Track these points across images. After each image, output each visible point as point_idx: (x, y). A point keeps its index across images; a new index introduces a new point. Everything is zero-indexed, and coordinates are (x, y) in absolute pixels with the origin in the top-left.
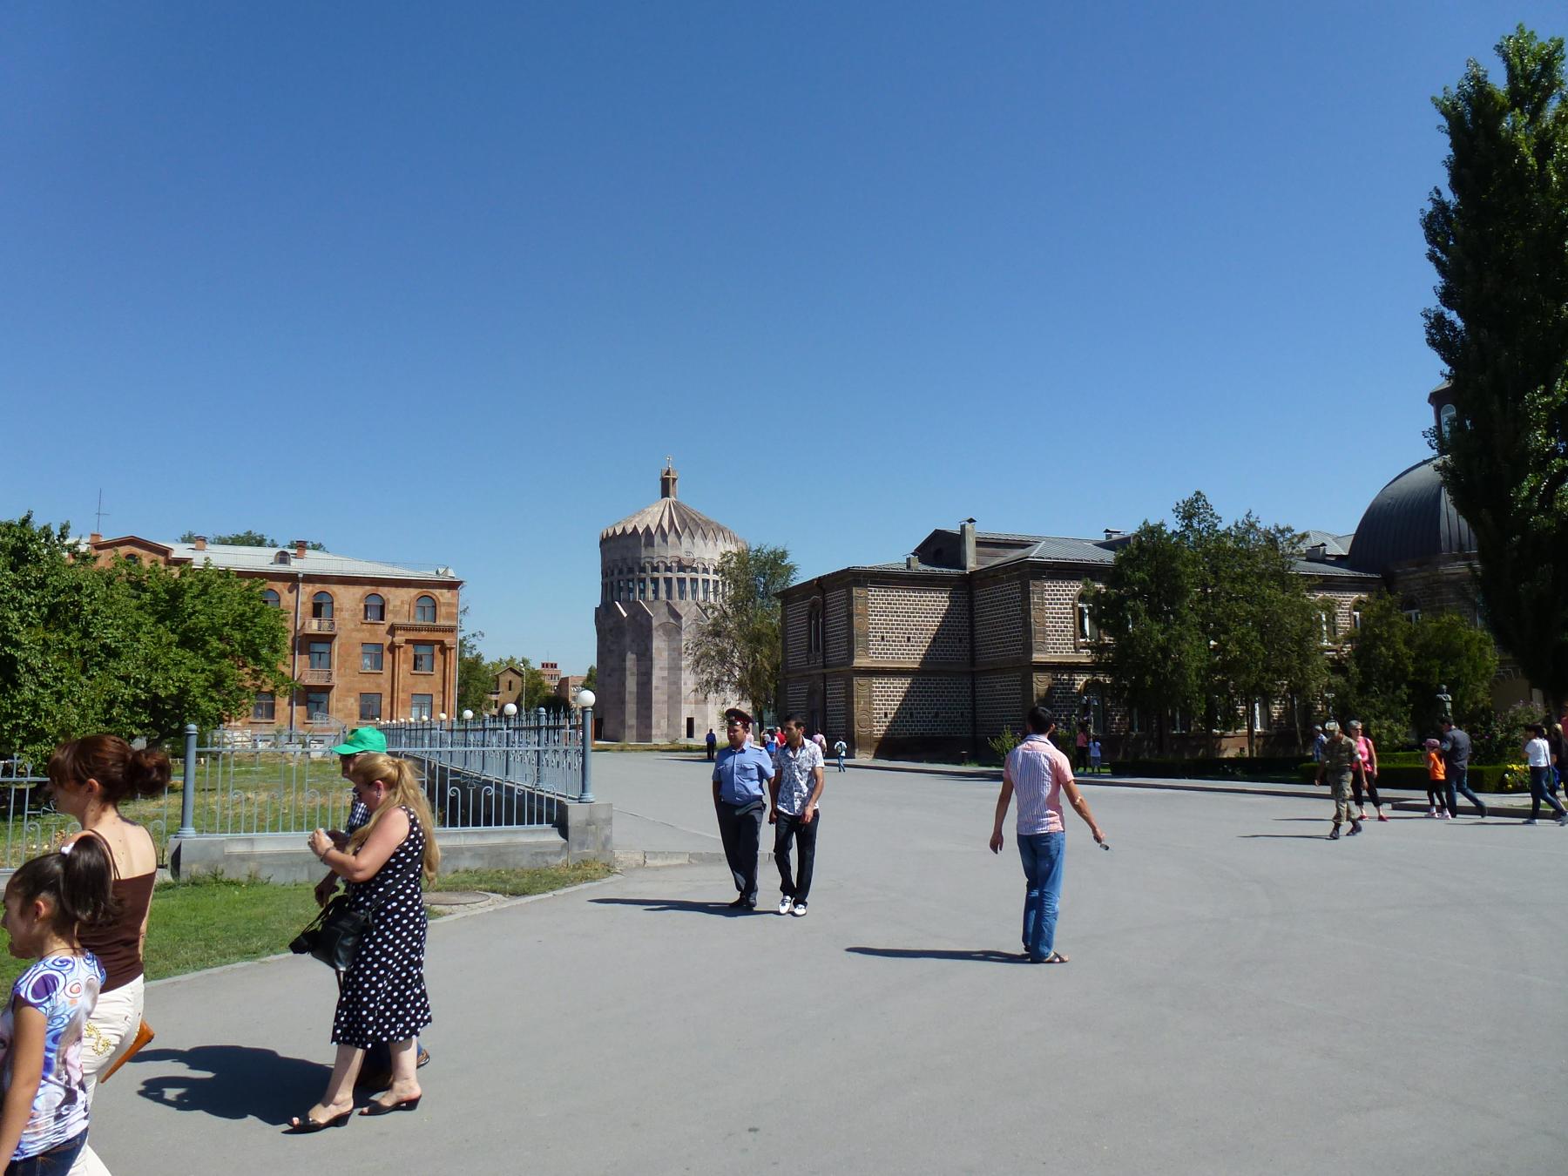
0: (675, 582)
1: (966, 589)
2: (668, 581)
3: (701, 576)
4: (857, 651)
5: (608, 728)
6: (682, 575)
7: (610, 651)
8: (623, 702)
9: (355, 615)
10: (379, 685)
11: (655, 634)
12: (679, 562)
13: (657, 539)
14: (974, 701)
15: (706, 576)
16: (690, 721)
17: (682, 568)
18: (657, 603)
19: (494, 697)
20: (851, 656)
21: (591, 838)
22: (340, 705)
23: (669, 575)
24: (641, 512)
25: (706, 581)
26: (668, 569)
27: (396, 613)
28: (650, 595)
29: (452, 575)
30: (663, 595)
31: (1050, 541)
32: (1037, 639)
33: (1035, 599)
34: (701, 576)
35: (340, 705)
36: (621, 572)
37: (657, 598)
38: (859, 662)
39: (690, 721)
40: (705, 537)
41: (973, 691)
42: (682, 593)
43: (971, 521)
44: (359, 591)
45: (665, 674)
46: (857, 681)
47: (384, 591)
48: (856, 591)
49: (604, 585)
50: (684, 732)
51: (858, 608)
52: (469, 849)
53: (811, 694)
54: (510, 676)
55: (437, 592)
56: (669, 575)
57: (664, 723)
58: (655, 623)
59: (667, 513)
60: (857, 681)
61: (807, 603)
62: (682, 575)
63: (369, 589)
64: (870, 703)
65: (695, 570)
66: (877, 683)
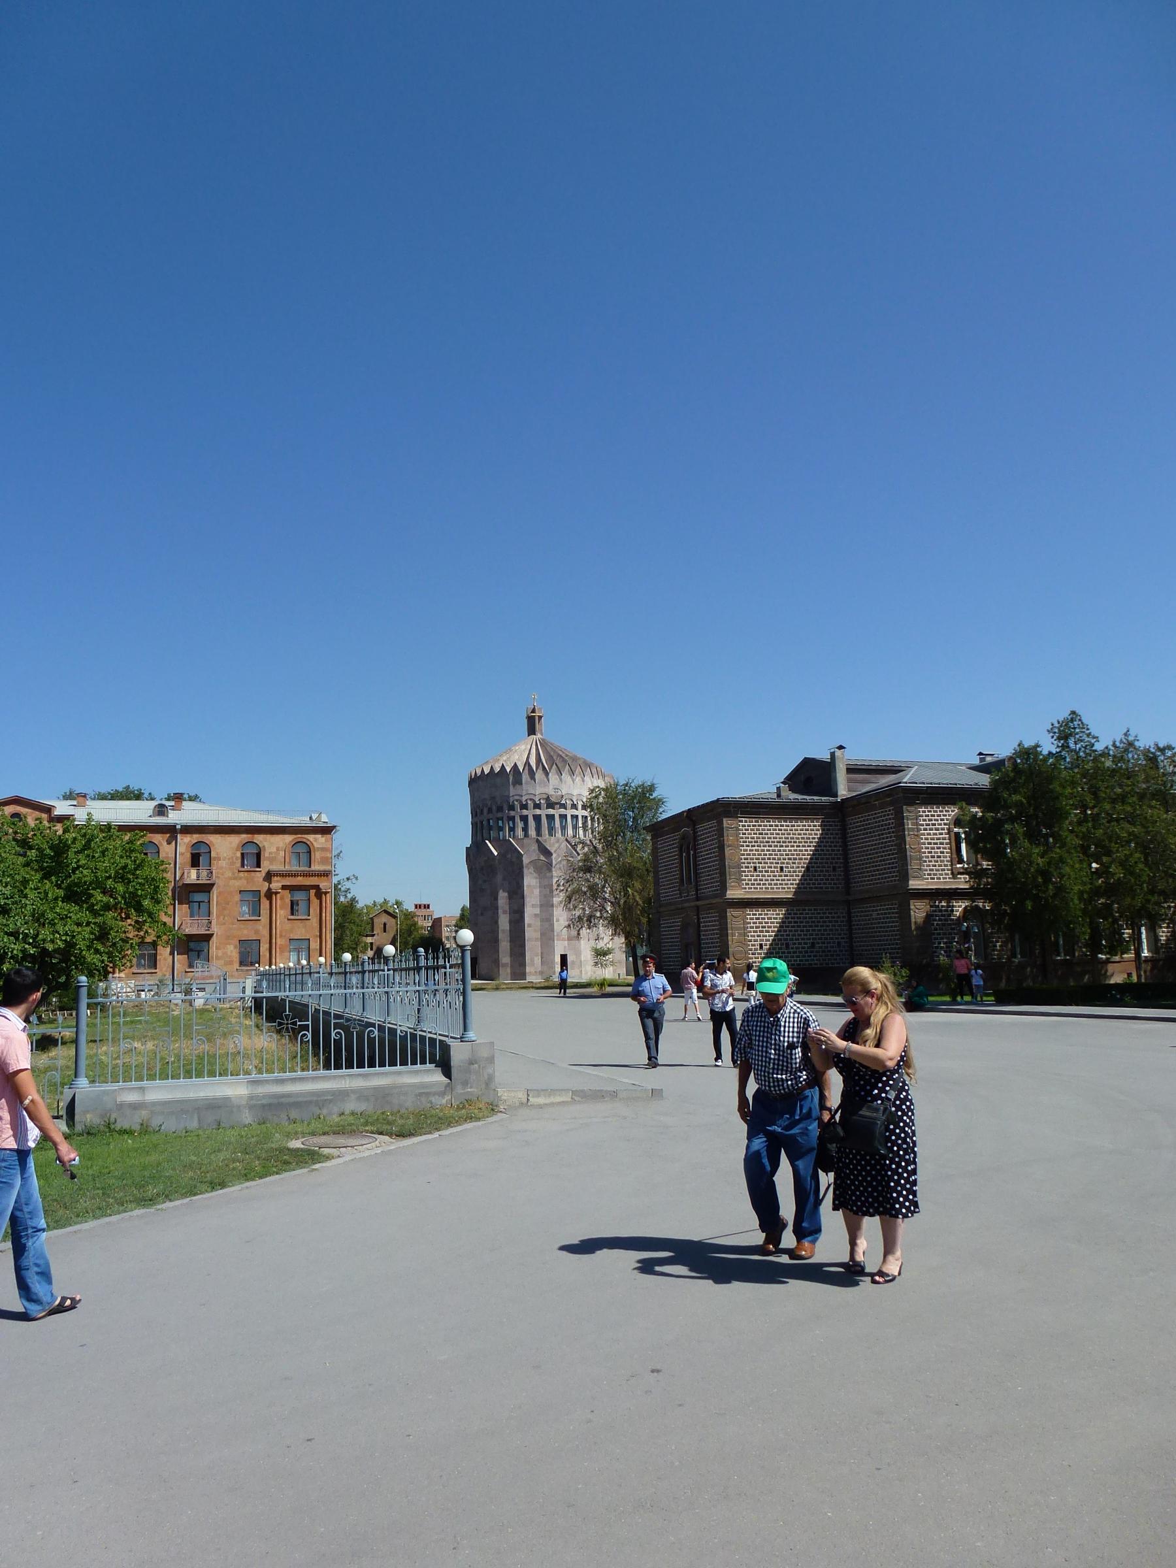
0: (544, 820)
1: (838, 817)
2: (537, 818)
3: (570, 812)
4: (730, 882)
5: (483, 967)
6: (551, 811)
8: (496, 941)
9: (233, 863)
10: (257, 932)
11: (525, 871)
12: (548, 799)
13: (525, 777)
14: (850, 930)
15: (575, 812)
16: (564, 958)
17: (551, 805)
18: (526, 841)
19: (369, 940)
20: (724, 888)
21: (473, 1077)
22: (220, 953)
23: (538, 812)
24: (509, 750)
25: (575, 817)
26: (537, 806)
27: (272, 860)
28: (520, 833)
29: (325, 819)
30: (532, 832)
31: (922, 765)
32: (913, 866)
33: (909, 825)
34: (570, 812)
35: (220, 953)
36: (490, 811)
37: (526, 835)
38: (733, 893)
39: (564, 958)
40: (572, 773)
41: (850, 921)
43: (841, 747)
44: (235, 840)
45: (537, 911)
46: (731, 913)
47: (259, 839)
48: (727, 822)
49: (474, 824)
51: (729, 839)
52: (354, 1091)
53: (685, 927)
54: (385, 918)
55: (311, 837)
56: (538, 812)
57: (537, 960)
58: (526, 860)
59: (534, 751)
60: (731, 913)
61: (677, 835)
62: (551, 811)
63: (245, 837)
64: (745, 935)
65: (564, 806)
66: (751, 914)
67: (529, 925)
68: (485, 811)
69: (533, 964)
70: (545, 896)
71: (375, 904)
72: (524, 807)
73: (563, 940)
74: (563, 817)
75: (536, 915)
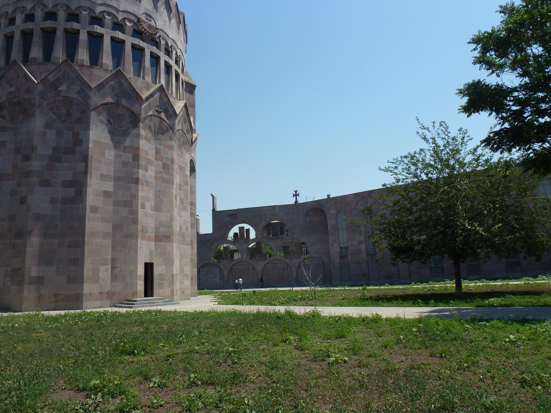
16: (149, 267)
26: (118, 26)
30: (107, 59)
34: (163, 58)
36: (30, 18)
39: (149, 267)
42: (139, 71)
45: (109, 186)
50: (141, 287)
57: (105, 272)
67: (94, 209)
69: (95, 279)
70: (125, 164)
72: (97, 20)
73: (149, 240)
74: (155, 59)
75: (106, 194)
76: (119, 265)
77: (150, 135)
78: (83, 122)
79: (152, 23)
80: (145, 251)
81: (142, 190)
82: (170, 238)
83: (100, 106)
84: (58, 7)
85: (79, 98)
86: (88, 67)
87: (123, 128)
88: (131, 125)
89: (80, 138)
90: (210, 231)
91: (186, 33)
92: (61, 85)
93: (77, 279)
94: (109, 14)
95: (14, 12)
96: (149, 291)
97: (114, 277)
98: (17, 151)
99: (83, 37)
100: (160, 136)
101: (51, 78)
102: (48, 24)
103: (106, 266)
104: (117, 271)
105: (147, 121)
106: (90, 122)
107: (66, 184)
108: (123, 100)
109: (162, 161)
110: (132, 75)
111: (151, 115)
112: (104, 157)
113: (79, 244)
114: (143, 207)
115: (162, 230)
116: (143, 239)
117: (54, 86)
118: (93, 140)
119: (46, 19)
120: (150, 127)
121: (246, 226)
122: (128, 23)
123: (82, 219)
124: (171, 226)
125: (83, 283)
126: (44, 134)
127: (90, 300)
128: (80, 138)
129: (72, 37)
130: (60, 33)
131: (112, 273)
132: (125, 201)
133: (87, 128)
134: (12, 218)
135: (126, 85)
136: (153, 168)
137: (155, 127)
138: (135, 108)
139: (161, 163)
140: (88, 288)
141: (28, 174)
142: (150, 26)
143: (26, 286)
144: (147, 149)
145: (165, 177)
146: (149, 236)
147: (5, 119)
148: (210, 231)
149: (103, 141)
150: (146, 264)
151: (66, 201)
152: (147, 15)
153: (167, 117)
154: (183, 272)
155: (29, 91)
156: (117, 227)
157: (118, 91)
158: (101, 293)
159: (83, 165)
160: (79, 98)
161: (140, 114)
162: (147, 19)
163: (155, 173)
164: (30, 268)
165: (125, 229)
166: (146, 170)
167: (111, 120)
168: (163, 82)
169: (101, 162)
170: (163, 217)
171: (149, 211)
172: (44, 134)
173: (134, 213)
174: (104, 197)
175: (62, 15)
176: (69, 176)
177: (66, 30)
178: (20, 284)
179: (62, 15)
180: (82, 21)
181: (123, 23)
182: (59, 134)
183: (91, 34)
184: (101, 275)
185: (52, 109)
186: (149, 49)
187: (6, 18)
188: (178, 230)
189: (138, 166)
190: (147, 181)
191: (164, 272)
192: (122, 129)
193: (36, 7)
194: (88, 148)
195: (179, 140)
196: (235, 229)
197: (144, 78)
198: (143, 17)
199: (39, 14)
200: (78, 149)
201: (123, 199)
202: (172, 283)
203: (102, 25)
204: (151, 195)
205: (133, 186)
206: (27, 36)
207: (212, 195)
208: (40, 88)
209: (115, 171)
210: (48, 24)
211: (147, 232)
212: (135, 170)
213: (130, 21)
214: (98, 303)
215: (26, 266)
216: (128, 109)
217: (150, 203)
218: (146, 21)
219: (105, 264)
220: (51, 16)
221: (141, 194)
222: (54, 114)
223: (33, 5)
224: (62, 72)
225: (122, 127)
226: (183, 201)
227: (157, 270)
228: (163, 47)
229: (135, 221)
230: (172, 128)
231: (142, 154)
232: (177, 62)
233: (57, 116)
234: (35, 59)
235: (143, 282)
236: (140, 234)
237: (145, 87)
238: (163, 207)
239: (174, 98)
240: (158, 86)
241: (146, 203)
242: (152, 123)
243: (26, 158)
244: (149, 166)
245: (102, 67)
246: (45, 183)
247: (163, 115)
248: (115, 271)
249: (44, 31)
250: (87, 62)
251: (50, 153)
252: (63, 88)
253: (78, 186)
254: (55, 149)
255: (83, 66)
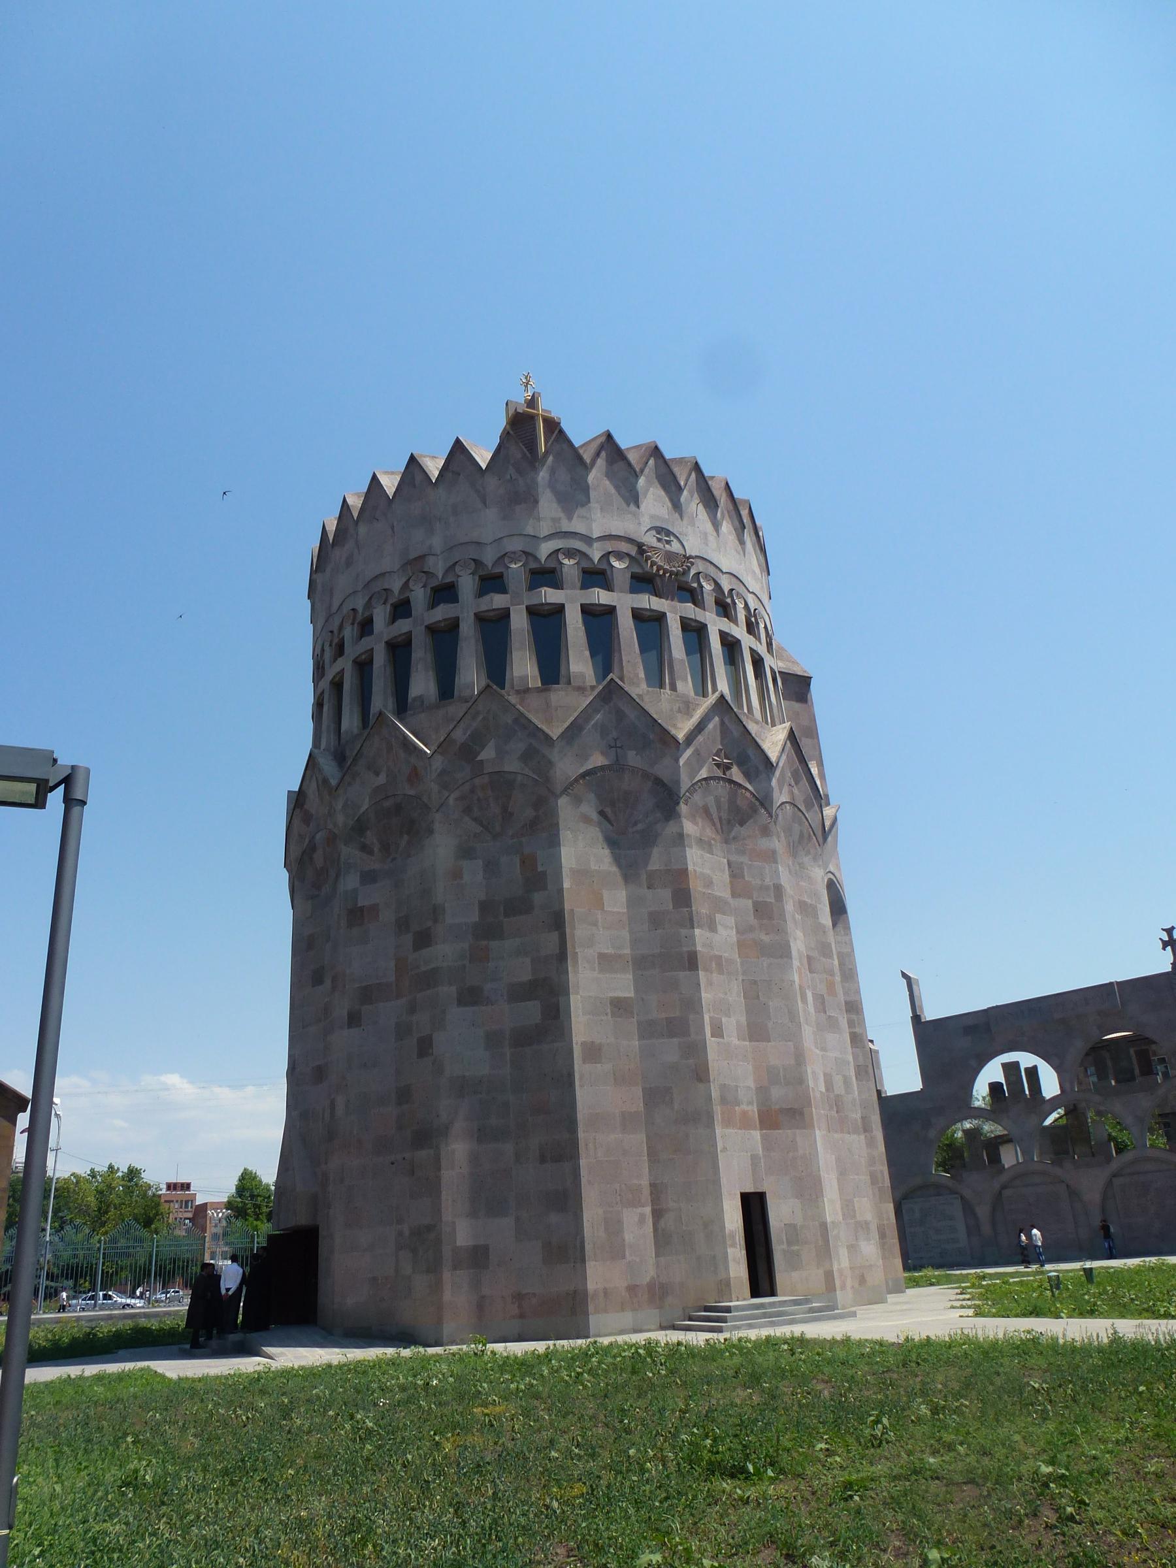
2: (599, 619)
6: (649, 602)
7: (357, 915)
16: (754, 1207)
26: (596, 576)
30: (579, 662)
34: (715, 625)
39: (754, 1207)
42: (659, 673)
45: (623, 985)
50: (737, 1267)
57: (637, 1228)
67: (593, 1052)
68: (380, 616)
69: (615, 1250)
70: (656, 920)
71: (93, 1174)
72: (546, 575)
73: (745, 1124)
74: (695, 632)
75: (619, 1006)
76: (671, 1204)
77: (709, 833)
78: (544, 827)
79: (675, 547)
80: (738, 1159)
81: (710, 983)
82: (802, 1114)
83: (576, 780)
84: (457, 568)
85: (527, 771)
86: (538, 690)
87: (640, 827)
88: (658, 815)
89: (540, 869)
90: (914, 1084)
91: (763, 550)
92: (483, 747)
93: (568, 1251)
94: (570, 553)
95: (368, 605)
96: (762, 1280)
97: (662, 1240)
98: (402, 924)
99: (519, 621)
100: (737, 828)
101: (460, 736)
102: (441, 613)
103: (639, 1210)
104: (668, 1221)
105: (697, 798)
106: (558, 824)
107: (521, 993)
108: (631, 754)
109: (750, 897)
110: (644, 686)
111: (705, 779)
112: (603, 909)
113: (563, 1152)
114: (718, 1032)
115: (777, 1093)
116: (728, 1123)
117: (468, 752)
118: (571, 869)
119: (433, 605)
120: (706, 811)
121: (1026, 1060)
122: (616, 564)
123: (567, 1081)
124: (801, 1081)
125: (583, 1261)
126: (456, 874)
127: (606, 1311)
128: (540, 869)
129: (494, 628)
130: (468, 629)
131: (655, 1230)
132: (669, 1021)
133: (554, 842)
134: (404, 1095)
135: (632, 715)
136: (731, 921)
137: (719, 808)
138: (661, 770)
139: (749, 903)
140: (598, 1275)
141: (430, 979)
142: (670, 556)
143: (447, 1275)
144: (707, 871)
145: (766, 938)
146: (744, 1113)
147: (371, 853)
148: (914, 1084)
149: (594, 866)
150: (746, 1198)
151: (525, 1038)
152: (659, 530)
153: (747, 775)
154: (854, 1216)
155: (414, 776)
156: (655, 1097)
157: (615, 734)
158: (632, 1289)
159: (555, 936)
160: (527, 771)
161: (677, 782)
162: (659, 540)
163: (738, 932)
164: (454, 1223)
165: (677, 1100)
166: (712, 927)
167: (608, 810)
168: (723, 686)
169: (595, 924)
170: (776, 1054)
171: (736, 1042)
172: (456, 874)
173: (695, 1051)
174: (613, 1015)
175: (467, 584)
176: (522, 970)
177: (480, 618)
178: (434, 1268)
179: (467, 584)
180: (511, 586)
181: (604, 566)
182: (491, 867)
183: (534, 612)
184: (628, 1237)
185: (468, 810)
186: (674, 611)
187: (353, 624)
188: (823, 1090)
189: (691, 920)
190: (719, 958)
191: (799, 1220)
192: (635, 829)
193: (411, 583)
194: (561, 891)
195: (788, 831)
196: (992, 1072)
197: (673, 688)
198: (650, 540)
199: (419, 596)
200: (538, 898)
201: (664, 1015)
202: (825, 1251)
203: (557, 584)
204: (734, 995)
205: (682, 975)
206: (399, 650)
207: (904, 975)
208: (438, 764)
209: (634, 942)
210: (441, 613)
211: (738, 1103)
212: (684, 932)
213: (620, 556)
214: (627, 1318)
215: (444, 1219)
216: (646, 775)
217: (733, 1020)
218: (660, 545)
219: (635, 1203)
220: (445, 593)
221: (706, 996)
222: (475, 819)
223: (404, 580)
224: (481, 717)
225: (636, 824)
226: (823, 1003)
227: (780, 1214)
228: (709, 600)
229: (701, 1074)
230: (764, 801)
231: (696, 886)
232: (751, 628)
233: (481, 825)
234: (420, 698)
235: (744, 1252)
236: (718, 1110)
237: (679, 711)
238: (770, 1025)
239: (757, 722)
240: (712, 699)
241: (724, 1020)
242: (711, 800)
243: (423, 940)
244: (718, 917)
245: (569, 683)
246: (471, 996)
247: (736, 774)
248: (662, 1224)
249: (481, 619)
250: (534, 681)
251: (474, 917)
252: (488, 753)
253: (548, 993)
254: (485, 907)
255: (527, 690)
